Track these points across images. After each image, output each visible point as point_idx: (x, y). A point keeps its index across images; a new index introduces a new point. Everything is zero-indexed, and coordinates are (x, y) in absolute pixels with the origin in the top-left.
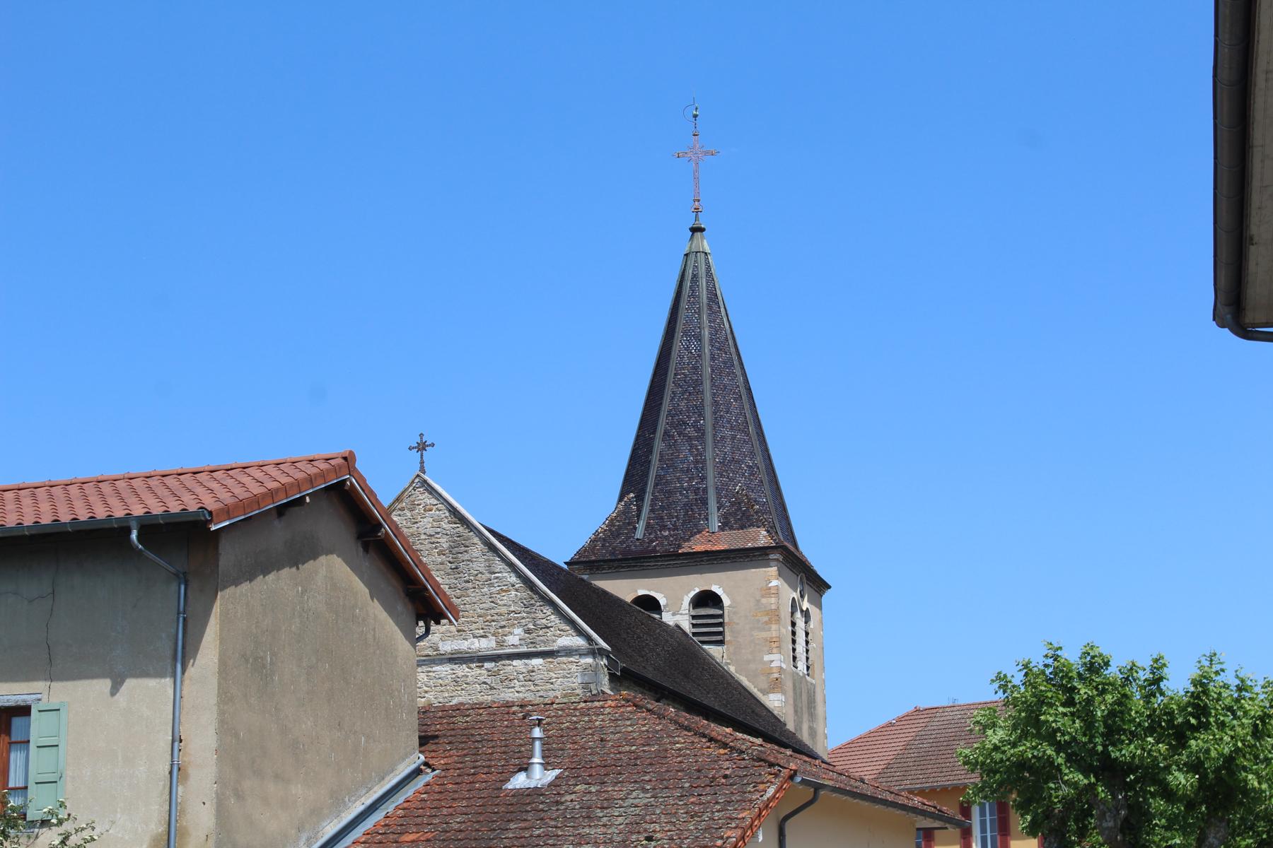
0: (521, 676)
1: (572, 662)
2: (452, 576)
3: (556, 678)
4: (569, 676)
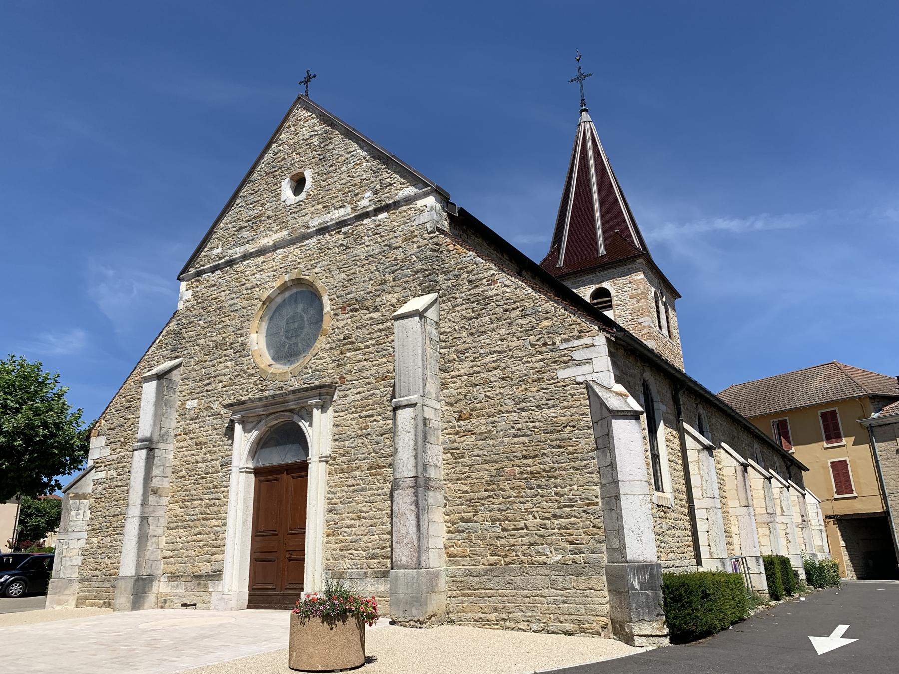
1: (411, 208)
2: (320, 165)
3: (397, 226)
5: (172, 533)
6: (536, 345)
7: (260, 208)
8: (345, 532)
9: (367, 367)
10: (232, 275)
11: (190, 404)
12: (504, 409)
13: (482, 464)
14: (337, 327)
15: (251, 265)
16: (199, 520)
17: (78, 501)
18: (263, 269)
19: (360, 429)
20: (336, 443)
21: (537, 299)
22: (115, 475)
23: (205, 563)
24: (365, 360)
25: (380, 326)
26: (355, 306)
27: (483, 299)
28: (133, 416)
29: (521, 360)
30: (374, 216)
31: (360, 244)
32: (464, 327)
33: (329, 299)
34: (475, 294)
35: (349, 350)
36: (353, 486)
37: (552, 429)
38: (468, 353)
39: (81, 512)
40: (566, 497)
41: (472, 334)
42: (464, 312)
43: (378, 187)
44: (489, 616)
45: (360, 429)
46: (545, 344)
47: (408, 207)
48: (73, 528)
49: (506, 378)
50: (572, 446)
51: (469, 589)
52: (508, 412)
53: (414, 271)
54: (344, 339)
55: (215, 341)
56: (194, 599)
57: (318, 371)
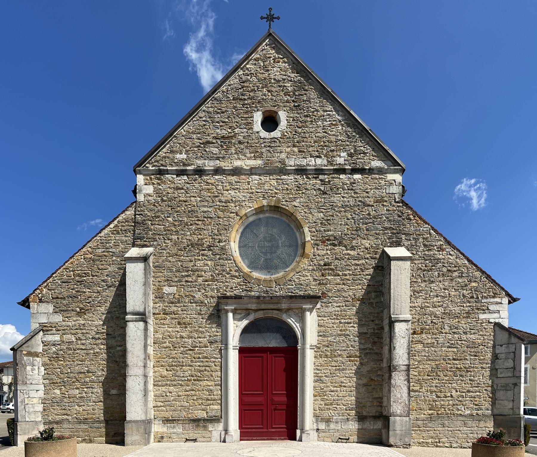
0: (345, 186)
1: (382, 178)
2: (296, 112)
3: (370, 189)
4: (379, 188)
5: (160, 389)
6: (466, 296)
7: (229, 131)
8: (330, 394)
9: (346, 289)
10: (202, 185)
11: (167, 290)
12: (443, 331)
13: (427, 361)
14: (319, 255)
15: (224, 181)
16: (190, 380)
17: (31, 358)
18: (237, 188)
19: (341, 330)
20: (320, 338)
21: (470, 268)
22: (74, 339)
23: (200, 411)
24: (344, 284)
25: (356, 262)
26: (334, 242)
27: (434, 260)
28: (89, 290)
29: (457, 304)
30: (350, 174)
31: (336, 194)
32: (420, 275)
33: (310, 231)
34: (428, 255)
35: (329, 275)
36: (336, 366)
37: (473, 346)
38: (421, 293)
39: (36, 368)
40: (475, 382)
41: (425, 281)
42: (420, 265)
43: (352, 151)
44: (427, 441)
45: (341, 330)
46: (472, 297)
47: (381, 177)
48: (31, 381)
49: (447, 313)
50: (483, 356)
51: (416, 427)
52: (446, 333)
53: (385, 228)
54: (325, 265)
55: (189, 240)
56: (192, 436)
57: (301, 285)
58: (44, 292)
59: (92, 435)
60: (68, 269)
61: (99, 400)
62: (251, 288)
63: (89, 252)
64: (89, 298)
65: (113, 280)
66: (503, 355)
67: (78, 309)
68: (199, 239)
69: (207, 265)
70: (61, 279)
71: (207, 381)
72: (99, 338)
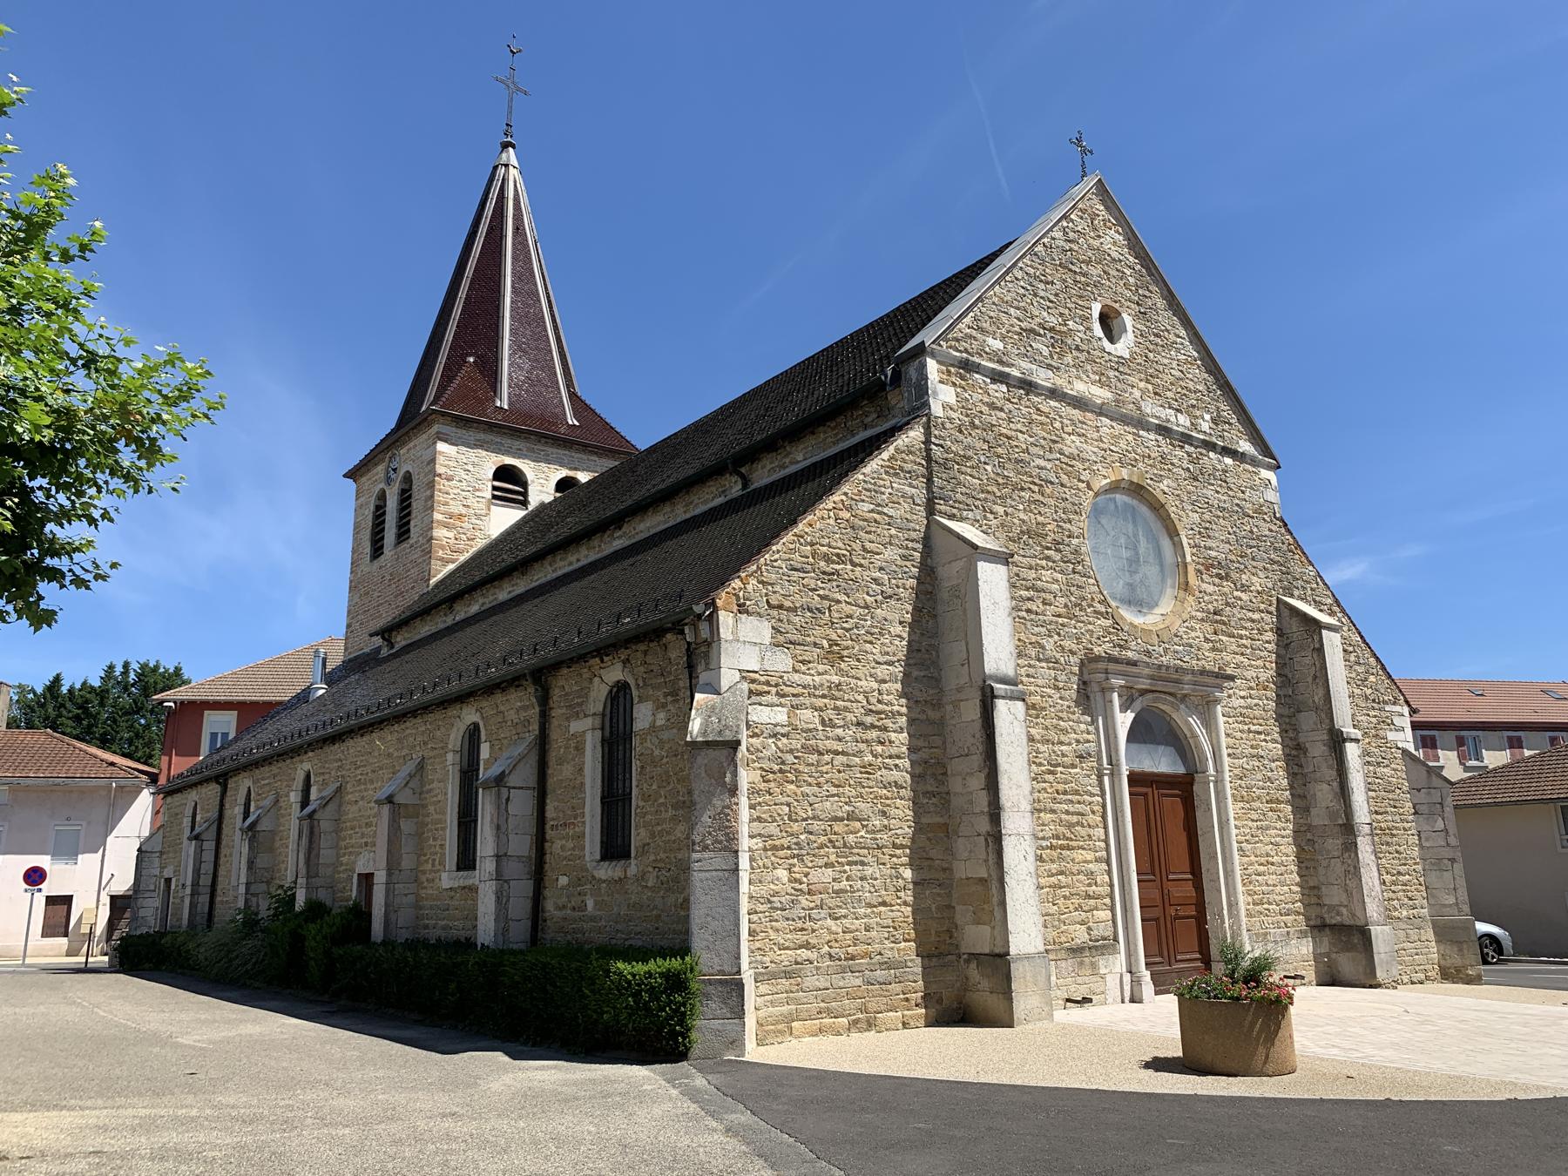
30: (1220, 454)
54: (1215, 613)
58: (750, 587)
59: (872, 1006)
60: (802, 537)
61: (880, 900)
62: (1126, 641)
63: (843, 504)
64: (847, 617)
65: (893, 581)
66: (1425, 807)
67: (826, 644)
68: (1038, 524)
69: (1057, 581)
70: (789, 560)
71: (1084, 849)
72: (873, 726)
